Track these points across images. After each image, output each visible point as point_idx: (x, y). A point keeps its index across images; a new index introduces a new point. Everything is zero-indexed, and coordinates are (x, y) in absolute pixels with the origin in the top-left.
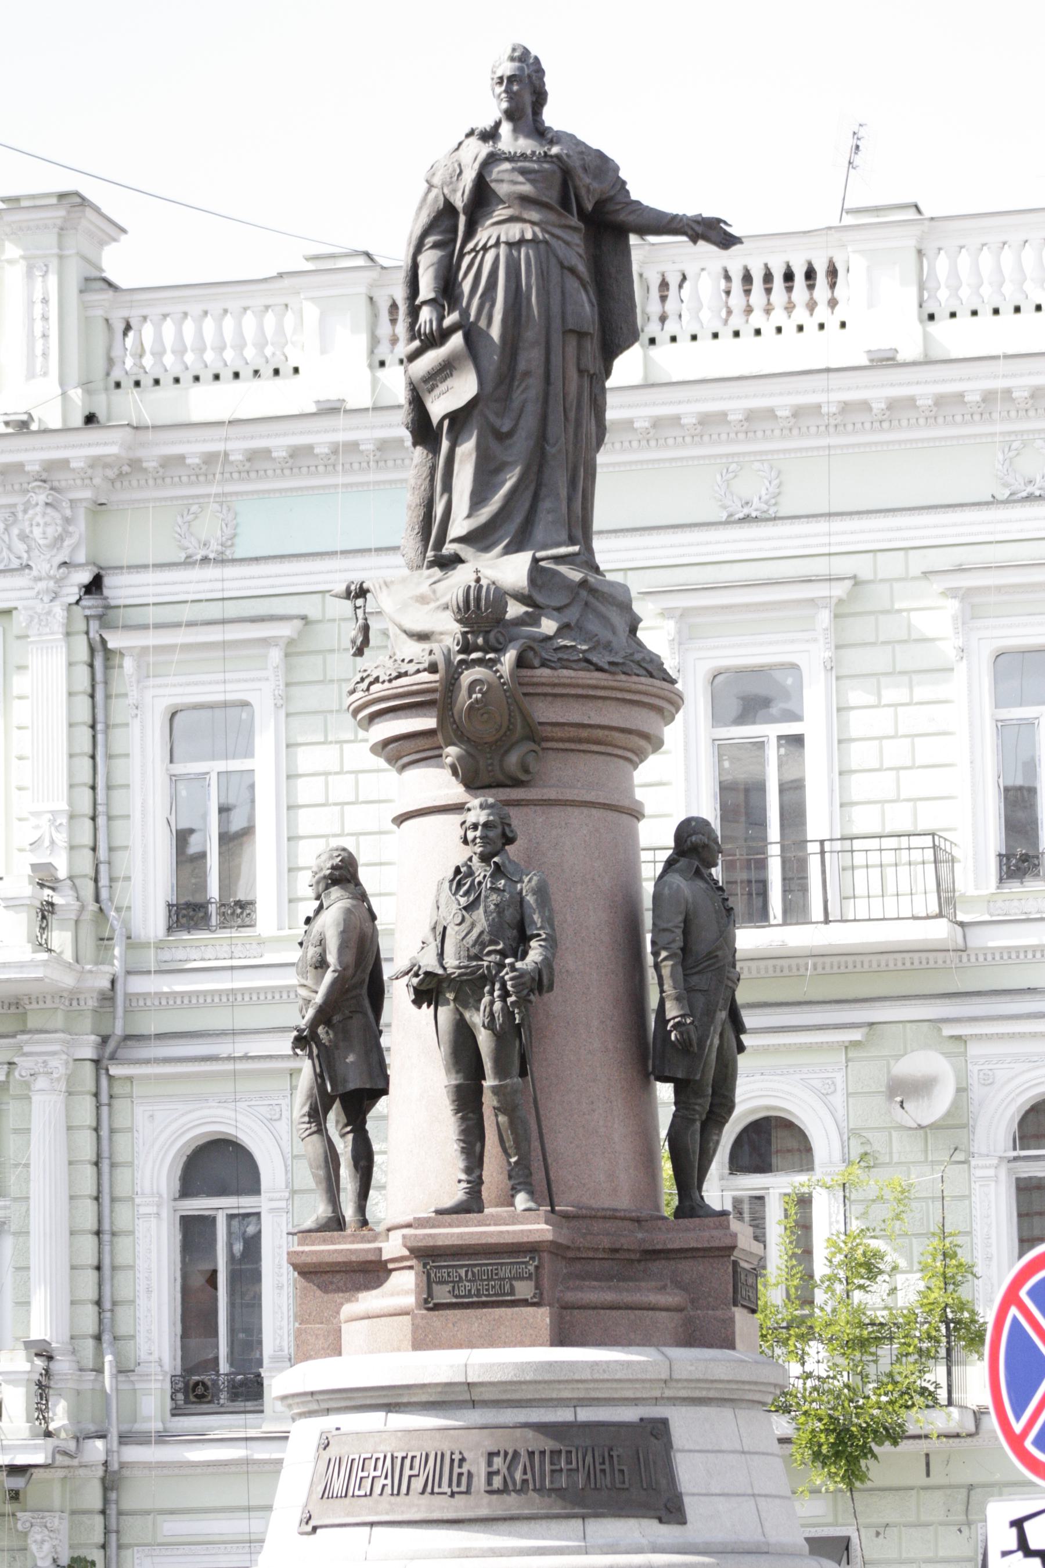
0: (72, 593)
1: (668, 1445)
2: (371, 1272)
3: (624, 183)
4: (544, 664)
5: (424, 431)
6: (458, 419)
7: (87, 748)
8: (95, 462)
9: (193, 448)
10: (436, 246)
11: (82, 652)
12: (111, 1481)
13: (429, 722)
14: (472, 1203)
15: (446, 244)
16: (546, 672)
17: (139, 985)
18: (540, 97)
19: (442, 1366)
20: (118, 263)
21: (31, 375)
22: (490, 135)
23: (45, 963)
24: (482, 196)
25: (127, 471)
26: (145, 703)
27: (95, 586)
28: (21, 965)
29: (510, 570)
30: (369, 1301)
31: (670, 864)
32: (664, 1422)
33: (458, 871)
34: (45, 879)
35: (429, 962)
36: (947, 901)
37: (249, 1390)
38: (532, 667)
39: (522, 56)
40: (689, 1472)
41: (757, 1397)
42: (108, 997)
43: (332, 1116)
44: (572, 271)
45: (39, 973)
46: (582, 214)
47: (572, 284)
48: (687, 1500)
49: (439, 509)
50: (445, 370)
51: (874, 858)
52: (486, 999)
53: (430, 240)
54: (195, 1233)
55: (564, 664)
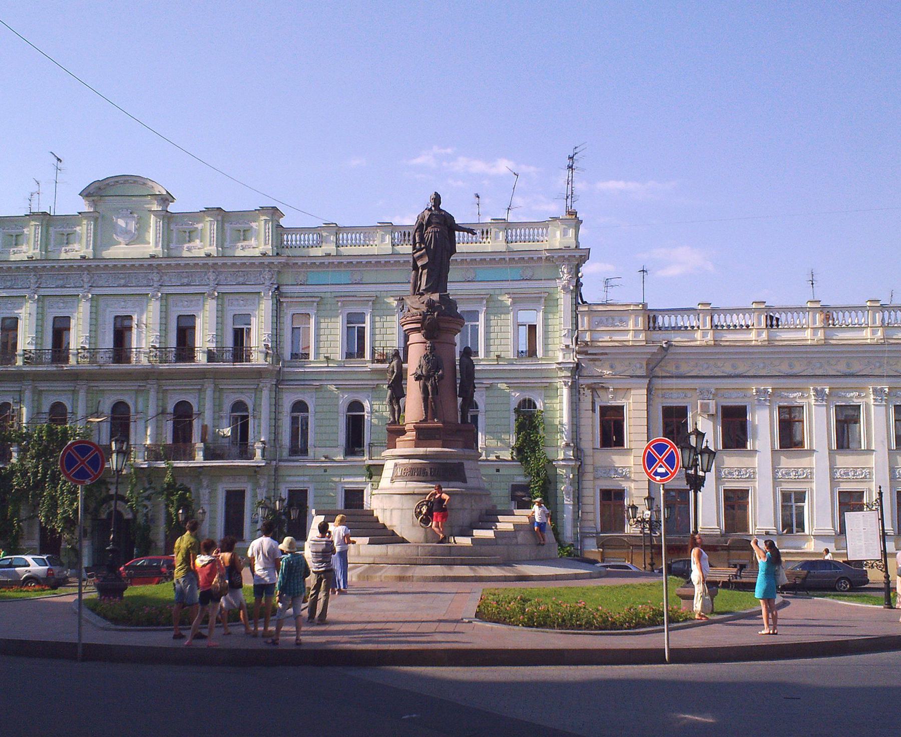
2: (403, 432)
5: (415, 268)
6: (423, 267)
9: (300, 261)
12: (276, 469)
13: (419, 325)
14: (425, 420)
15: (421, 231)
17: (286, 369)
19: (421, 450)
20: (283, 222)
21: (265, 244)
22: (430, 210)
24: (429, 223)
25: (286, 265)
26: (288, 313)
27: (277, 289)
29: (436, 297)
30: (402, 438)
37: (305, 452)
39: (436, 194)
40: (468, 474)
42: (279, 371)
50: (421, 257)
54: (294, 420)
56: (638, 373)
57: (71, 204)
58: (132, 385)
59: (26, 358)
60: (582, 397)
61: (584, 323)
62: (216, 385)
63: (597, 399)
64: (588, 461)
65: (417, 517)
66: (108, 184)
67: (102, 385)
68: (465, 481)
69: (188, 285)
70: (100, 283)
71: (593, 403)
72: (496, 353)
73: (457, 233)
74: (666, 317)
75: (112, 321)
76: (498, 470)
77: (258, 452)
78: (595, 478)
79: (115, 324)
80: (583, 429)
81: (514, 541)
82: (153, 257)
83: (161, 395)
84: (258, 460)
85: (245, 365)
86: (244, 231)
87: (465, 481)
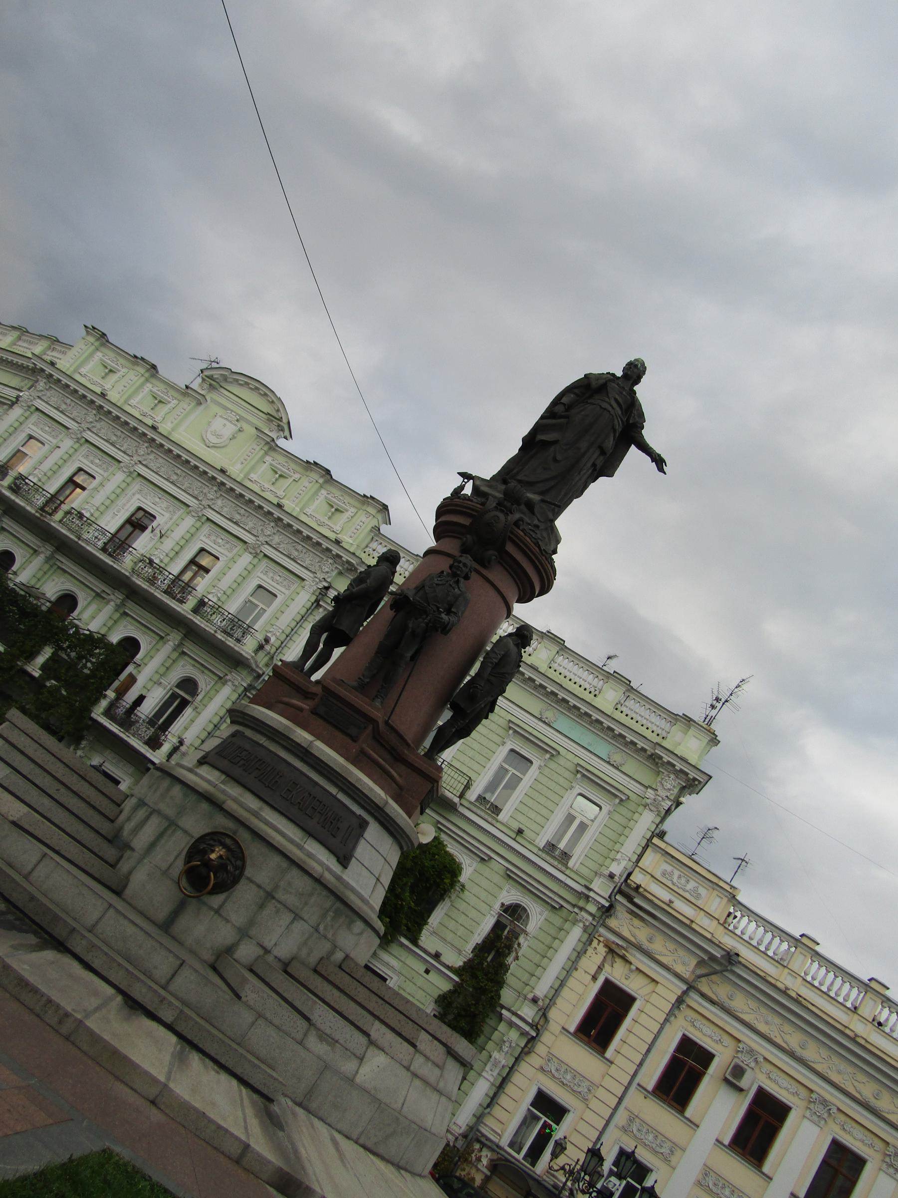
0: (321, 586)
1: (361, 835)
3: (643, 428)
4: (523, 531)
6: (546, 444)
7: (298, 620)
8: (348, 562)
10: (575, 394)
11: (313, 598)
13: (466, 521)
16: (522, 533)
18: (637, 380)
20: (384, 529)
23: (252, 657)
28: (247, 653)
31: (510, 635)
32: (367, 823)
33: (442, 572)
34: (267, 640)
35: (411, 595)
36: (461, 796)
38: (519, 528)
40: (362, 851)
41: (403, 844)
43: (324, 636)
44: (615, 431)
45: (249, 657)
46: (628, 420)
47: (612, 435)
48: (353, 860)
49: (515, 471)
51: (452, 775)
52: (420, 620)
53: (576, 391)
55: (530, 537)
56: (679, 969)
57: (185, 374)
58: (99, 586)
59: (15, 484)
60: (590, 950)
61: (650, 860)
62: (181, 644)
63: (607, 967)
64: (546, 1037)
65: (189, 857)
66: (237, 380)
67: (68, 564)
68: (344, 861)
69: (236, 523)
70: (151, 465)
71: (600, 968)
72: (521, 826)
73: (633, 448)
74: (753, 924)
75: (133, 509)
76: (427, 972)
77: (166, 748)
78: (542, 1069)
79: (133, 515)
80: (565, 992)
81: (349, 1066)
82: (223, 471)
83: (117, 615)
84: (157, 757)
85: (231, 642)
86: (337, 510)
87: (344, 861)
